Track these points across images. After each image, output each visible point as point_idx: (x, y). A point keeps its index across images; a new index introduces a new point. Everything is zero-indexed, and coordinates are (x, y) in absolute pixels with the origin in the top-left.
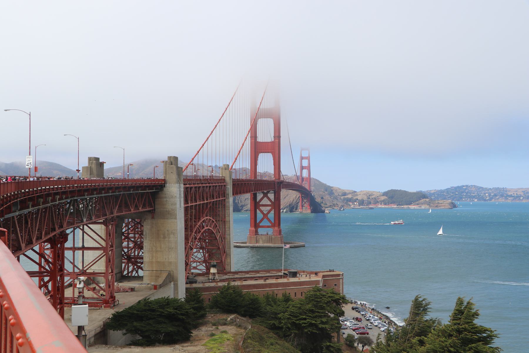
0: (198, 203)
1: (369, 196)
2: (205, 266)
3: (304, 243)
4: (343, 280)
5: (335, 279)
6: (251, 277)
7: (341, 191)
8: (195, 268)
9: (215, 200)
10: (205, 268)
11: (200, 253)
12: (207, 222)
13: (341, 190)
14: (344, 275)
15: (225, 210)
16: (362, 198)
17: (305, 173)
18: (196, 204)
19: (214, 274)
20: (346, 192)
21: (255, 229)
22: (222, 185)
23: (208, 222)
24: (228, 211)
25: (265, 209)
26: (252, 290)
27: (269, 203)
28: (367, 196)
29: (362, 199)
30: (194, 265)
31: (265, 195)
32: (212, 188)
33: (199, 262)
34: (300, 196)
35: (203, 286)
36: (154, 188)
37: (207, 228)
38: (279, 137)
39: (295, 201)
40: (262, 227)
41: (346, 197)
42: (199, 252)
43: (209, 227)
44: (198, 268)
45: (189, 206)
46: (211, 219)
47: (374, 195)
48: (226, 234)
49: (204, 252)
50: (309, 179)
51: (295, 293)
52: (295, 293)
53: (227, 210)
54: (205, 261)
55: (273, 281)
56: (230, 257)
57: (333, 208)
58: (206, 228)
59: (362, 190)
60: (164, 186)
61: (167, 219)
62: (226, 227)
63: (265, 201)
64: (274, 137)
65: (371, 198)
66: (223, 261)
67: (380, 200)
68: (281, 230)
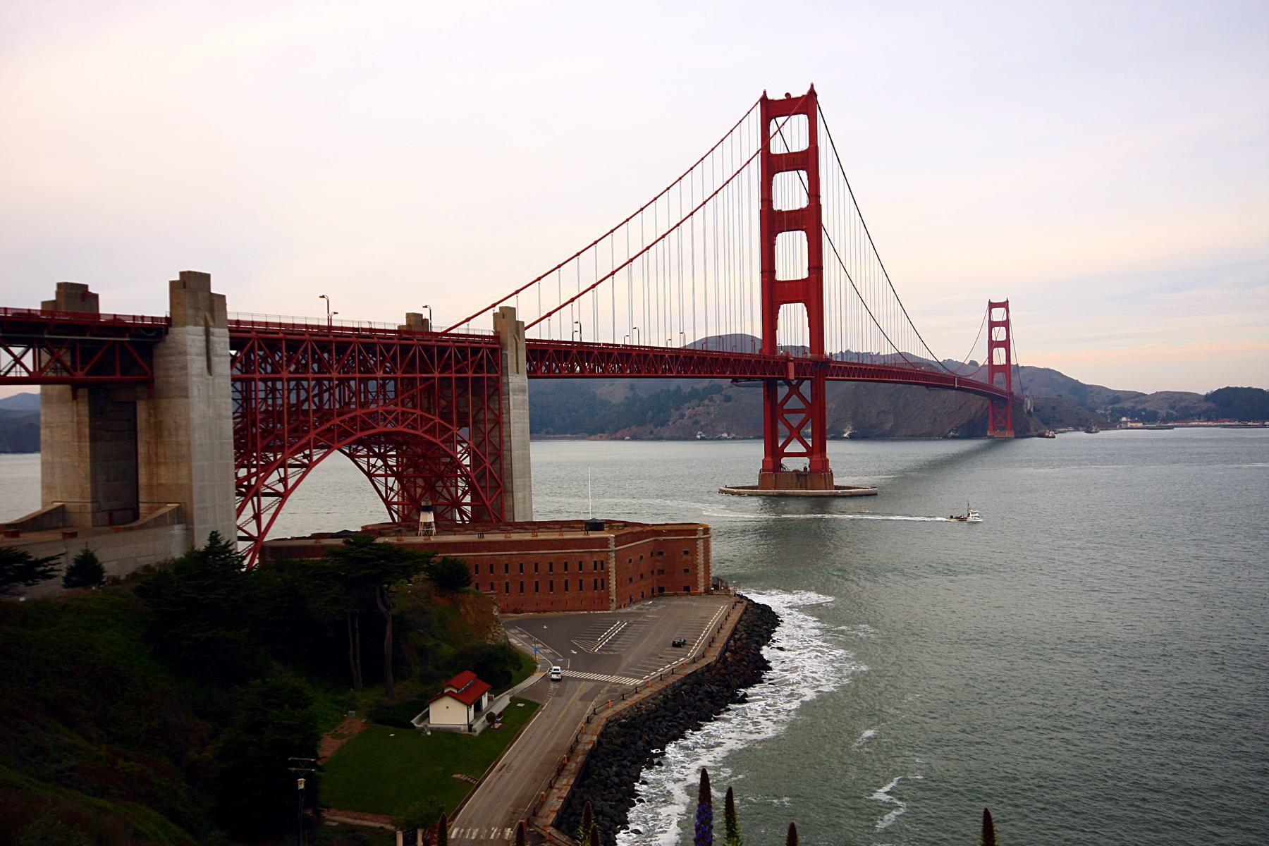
9: (436, 375)
17: (999, 357)
19: (428, 525)
21: (770, 459)
25: (795, 420)
27: (802, 406)
31: (794, 390)
36: (127, 335)
39: (979, 415)
41: (1117, 406)
50: (1007, 368)
51: (551, 564)
60: (167, 332)
61: (173, 397)
62: (504, 434)
63: (794, 402)
64: (809, 269)
67: (1198, 410)
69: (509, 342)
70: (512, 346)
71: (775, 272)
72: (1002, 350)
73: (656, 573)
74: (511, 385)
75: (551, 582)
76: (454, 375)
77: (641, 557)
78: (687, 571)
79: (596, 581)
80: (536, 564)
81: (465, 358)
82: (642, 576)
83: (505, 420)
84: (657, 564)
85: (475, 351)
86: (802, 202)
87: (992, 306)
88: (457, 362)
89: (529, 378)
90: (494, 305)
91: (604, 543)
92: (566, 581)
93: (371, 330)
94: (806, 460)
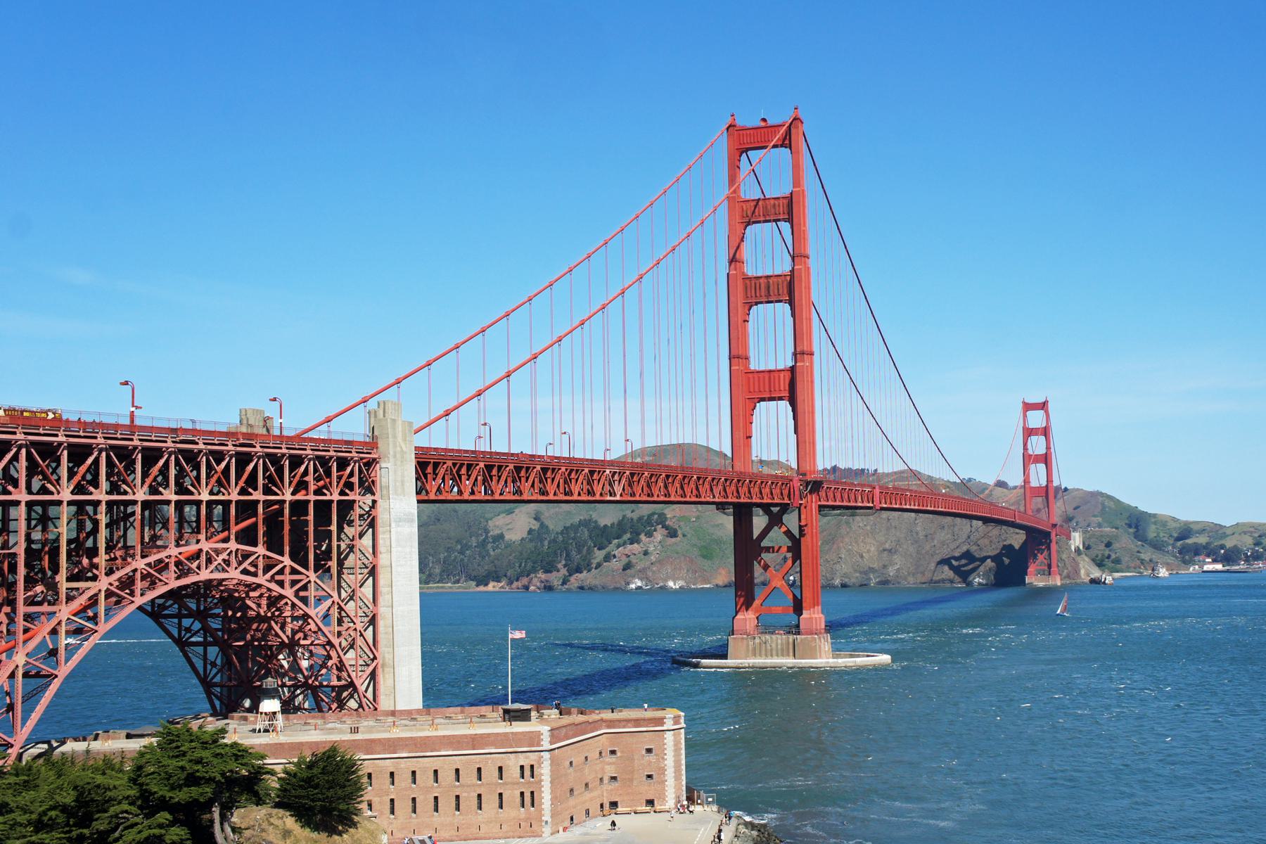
1: (1260, 536)
7: (1178, 525)
9: (288, 497)
17: (1038, 476)
20: (1192, 526)
28: (1254, 538)
31: (775, 520)
41: (1189, 541)
50: (1048, 492)
51: (457, 771)
52: (457, 771)
53: (384, 533)
64: (795, 354)
69: (391, 453)
70: (395, 456)
72: (1042, 467)
73: (606, 780)
74: (392, 513)
75: (458, 797)
76: (312, 497)
77: (586, 758)
78: (650, 776)
79: (522, 794)
80: (436, 772)
81: (328, 473)
82: (587, 785)
84: (607, 767)
85: (343, 464)
86: (783, 265)
87: (1028, 407)
88: (317, 479)
89: (419, 502)
90: (364, 401)
91: (534, 738)
92: (479, 796)
93: (195, 432)
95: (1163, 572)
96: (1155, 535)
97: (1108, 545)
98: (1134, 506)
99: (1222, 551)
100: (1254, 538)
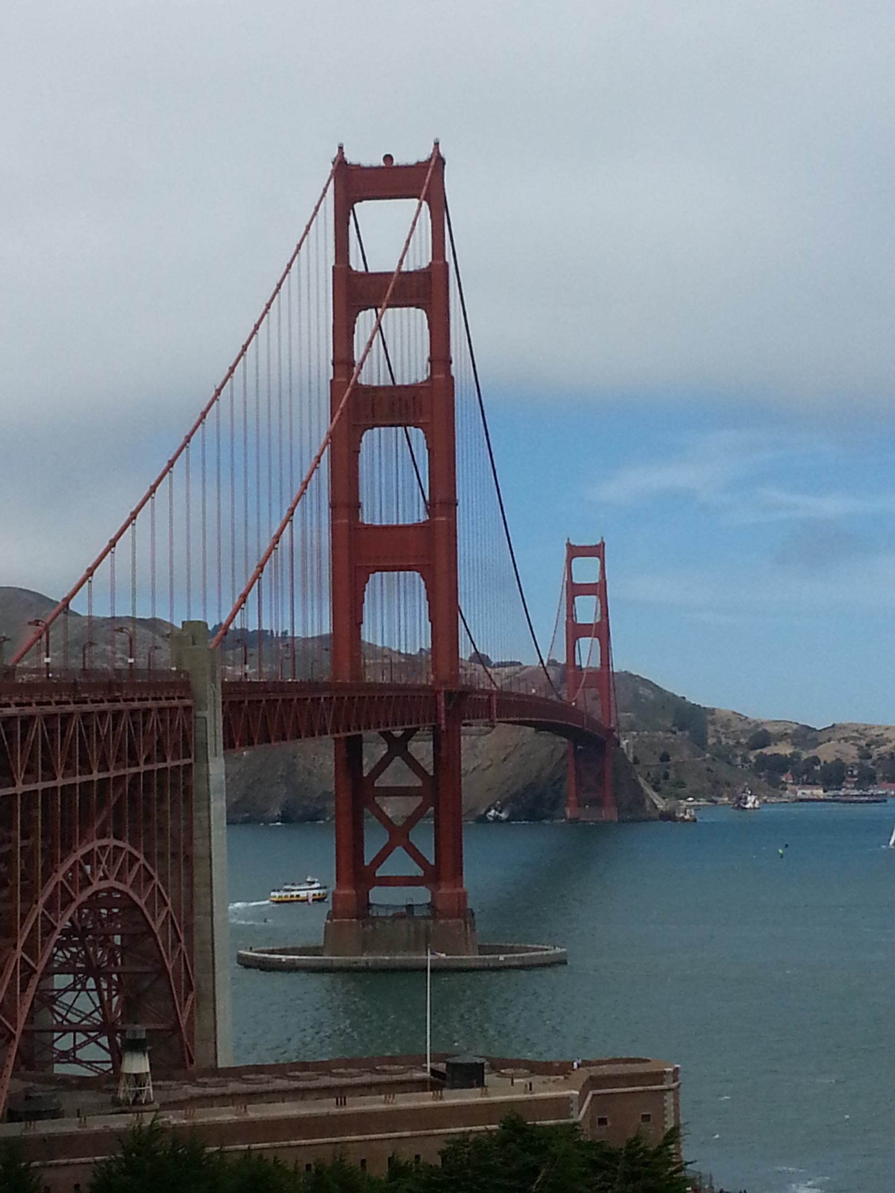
0: (60, 782)
2: (107, 1046)
3: (564, 950)
4: (676, 1097)
5: (643, 1091)
6: (297, 1090)
7: (748, 727)
8: (68, 1056)
9: (142, 768)
10: (108, 1057)
11: (87, 991)
12: (103, 860)
13: (750, 724)
14: (680, 1075)
15: (189, 810)
16: (839, 755)
18: (52, 784)
19: (138, 1079)
20: (768, 728)
21: (354, 892)
22: (177, 708)
23: (107, 862)
24: (206, 814)
26: (285, 1143)
28: (860, 748)
29: (838, 760)
30: (64, 1043)
32: (124, 720)
33: (85, 1032)
34: (567, 751)
35: (80, 1127)
37: (105, 884)
38: (451, 504)
40: (387, 881)
41: (768, 751)
42: (84, 989)
43: (112, 883)
44: (79, 1054)
45: (19, 793)
46: (123, 849)
47: (891, 741)
48: (196, 910)
49: (104, 986)
54: (107, 1028)
55: (374, 1104)
56: (212, 1005)
57: (712, 801)
58: (97, 885)
59: (837, 722)
62: (196, 880)
65: (875, 757)
66: (183, 1023)
68: (465, 894)
71: (359, 506)
74: (211, 783)
83: (199, 848)
87: (574, 552)
94: (421, 895)
95: (751, 801)
96: (714, 740)
97: (665, 758)
98: (680, 696)
99: (818, 768)
100: (860, 748)
